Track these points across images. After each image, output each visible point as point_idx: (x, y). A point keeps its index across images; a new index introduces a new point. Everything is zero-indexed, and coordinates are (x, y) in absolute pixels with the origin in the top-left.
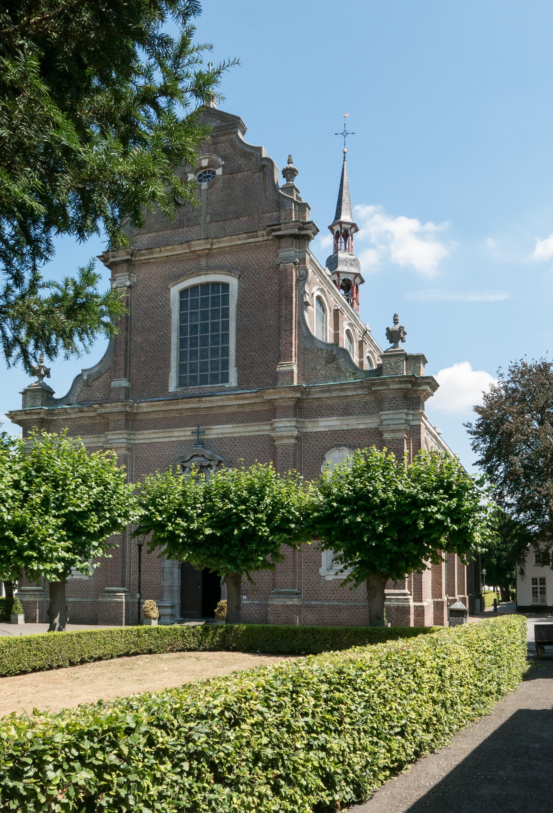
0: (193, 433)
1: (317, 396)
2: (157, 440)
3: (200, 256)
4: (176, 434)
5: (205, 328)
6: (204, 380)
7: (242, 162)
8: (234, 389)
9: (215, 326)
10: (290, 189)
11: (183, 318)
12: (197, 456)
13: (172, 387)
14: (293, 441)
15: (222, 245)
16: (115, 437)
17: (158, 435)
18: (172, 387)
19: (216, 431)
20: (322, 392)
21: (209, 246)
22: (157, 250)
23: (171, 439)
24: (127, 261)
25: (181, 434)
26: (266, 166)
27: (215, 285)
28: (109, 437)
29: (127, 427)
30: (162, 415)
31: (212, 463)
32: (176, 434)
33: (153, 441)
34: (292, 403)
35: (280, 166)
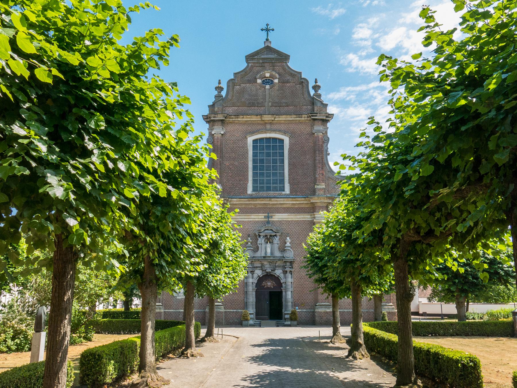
0: (265, 217)
3: (266, 123)
4: (252, 217)
6: (269, 189)
7: (289, 78)
8: (288, 195)
9: (275, 161)
11: (255, 155)
12: (268, 230)
13: (250, 191)
15: (281, 119)
17: (241, 217)
18: (250, 191)
21: (273, 119)
24: (222, 120)
26: (304, 83)
27: (275, 139)
30: (243, 206)
31: (278, 234)
32: (252, 217)
35: (311, 84)
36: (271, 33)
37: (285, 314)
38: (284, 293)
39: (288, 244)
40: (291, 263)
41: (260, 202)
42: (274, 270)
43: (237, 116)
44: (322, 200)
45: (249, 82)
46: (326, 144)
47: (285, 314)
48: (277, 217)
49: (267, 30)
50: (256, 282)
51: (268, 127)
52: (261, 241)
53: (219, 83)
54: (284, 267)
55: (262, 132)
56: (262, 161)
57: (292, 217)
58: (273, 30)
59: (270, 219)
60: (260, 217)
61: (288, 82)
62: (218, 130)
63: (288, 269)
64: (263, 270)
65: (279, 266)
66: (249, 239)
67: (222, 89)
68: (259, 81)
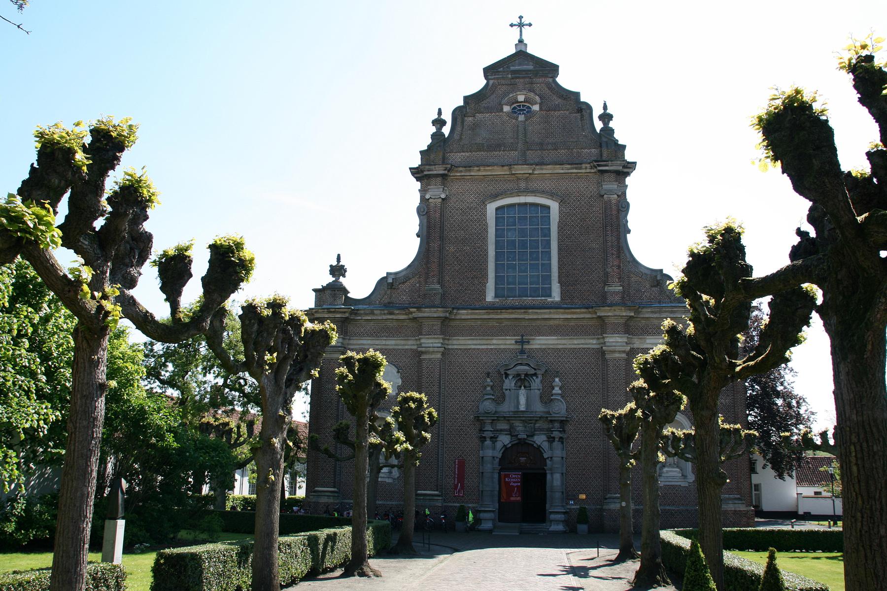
0: (516, 342)
1: (647, 316)
2: (473, 347)
3: (518, 179)
4: (494, 342)
5: (523, 244)
10: (608, 131)
11: (499, 233)
12: (521, 364)
13: (490, 297)
14: (624, 355)
15: (544, 172)
16: (430, 341)
17: (475, 342)
18: (490, 297)
19: (540, 342)
20: (652, 312)
21: (530, 172)
22: (476, 168)
23: (489, 347)
25: (500, 342)
28: (422, 341)
29: (442, 333)
31: (538, 372)
32: (494, 342)
33: (469, 347)
34: (622, 321)
35: (597, 111)
36: (526, 29)
37: (551, 513)
38: (549, 477)
39: (557, 390)
40: (563, 423)
41: (507, 316)
42: (532, 436)
43: (468, 166)
44: (617, 313)
45: (489, 110)
46: (623, 213)
47: (551, 513)
48: (538, 342)
49: (521, 25)
50: (500, 456)
51: (523, 185)
52: (509, 383)
53: (440, 112)
54: (550, 430)
55: (511, 195)
56: (512, 243)
57: (564, 342)
58: (530, 25)
59: (525, 347)
60: (508, 342)
61: (557, 108)
62: (437, 192)
63: (556, 434)
64: (512, 436)
65: (541, 430)
66: (489, 380)
67: (443, 123)
68: (506, 109)
